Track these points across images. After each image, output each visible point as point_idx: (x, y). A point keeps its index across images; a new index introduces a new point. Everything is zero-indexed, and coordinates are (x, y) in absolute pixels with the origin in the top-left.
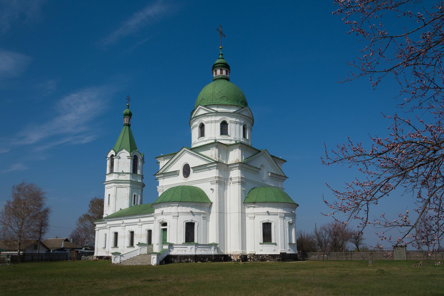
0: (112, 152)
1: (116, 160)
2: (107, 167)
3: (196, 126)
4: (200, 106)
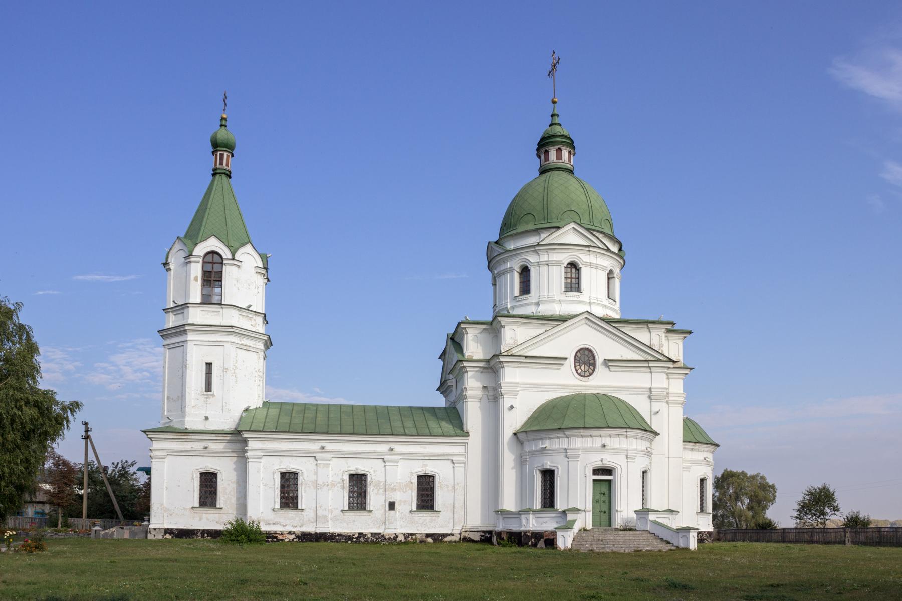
0: (213, 244)
1: (229, 273)
2: (193, 283)
3: (558, 263)
4: (572, 225)
